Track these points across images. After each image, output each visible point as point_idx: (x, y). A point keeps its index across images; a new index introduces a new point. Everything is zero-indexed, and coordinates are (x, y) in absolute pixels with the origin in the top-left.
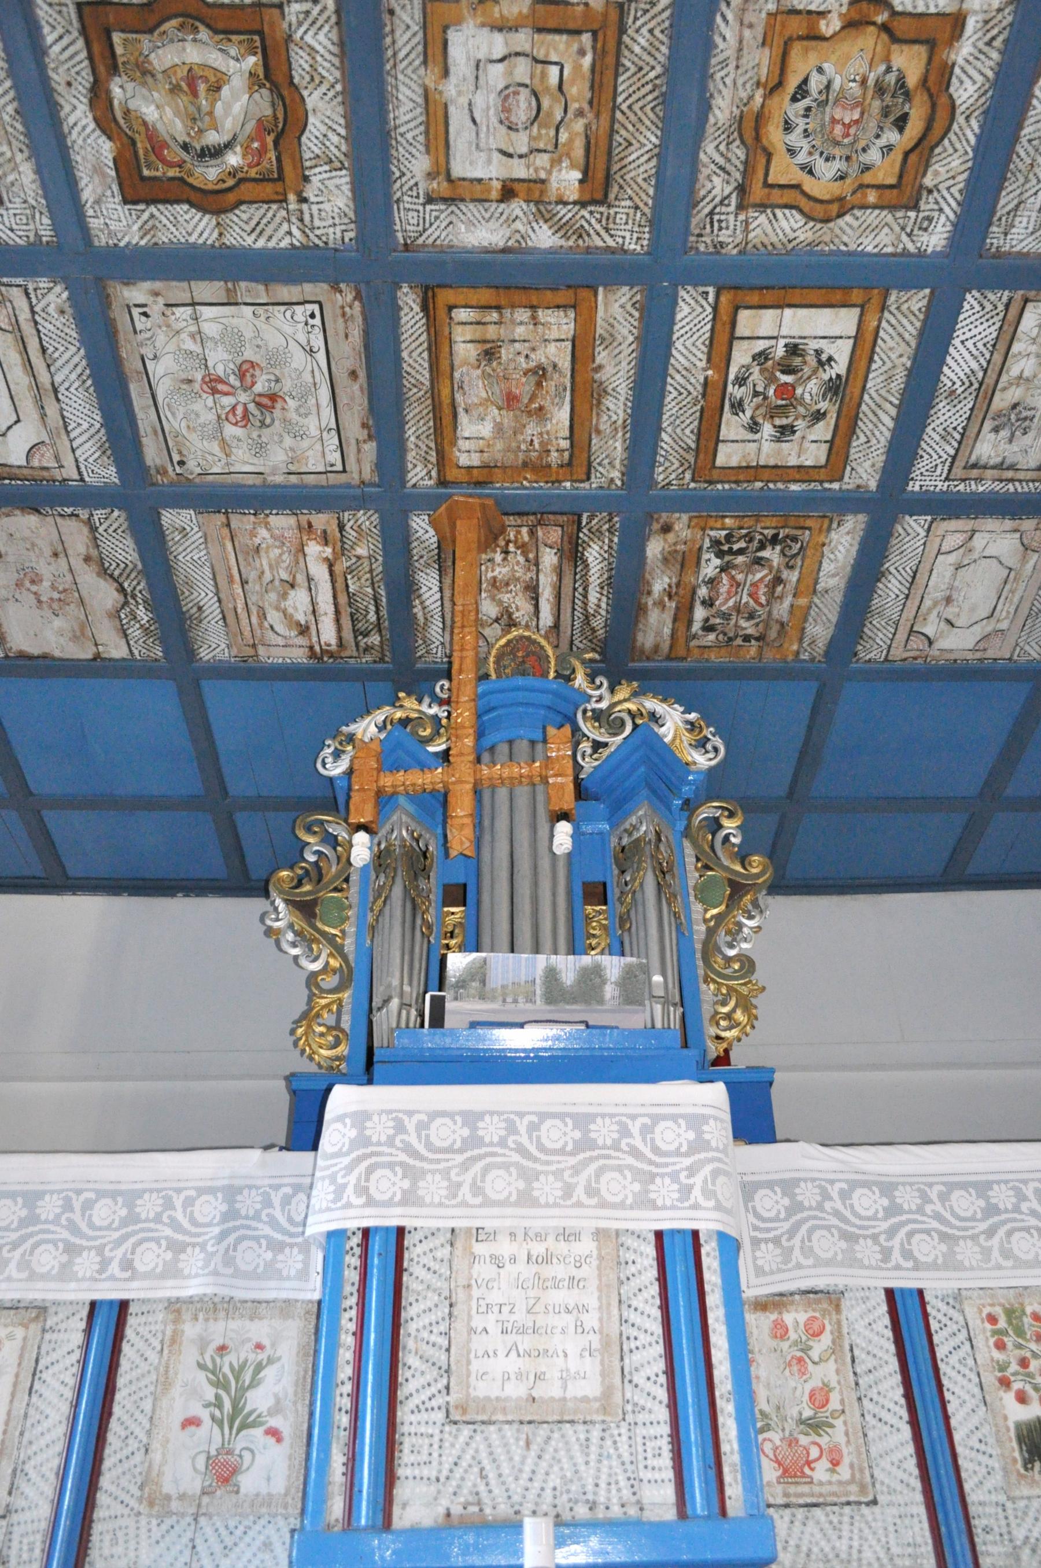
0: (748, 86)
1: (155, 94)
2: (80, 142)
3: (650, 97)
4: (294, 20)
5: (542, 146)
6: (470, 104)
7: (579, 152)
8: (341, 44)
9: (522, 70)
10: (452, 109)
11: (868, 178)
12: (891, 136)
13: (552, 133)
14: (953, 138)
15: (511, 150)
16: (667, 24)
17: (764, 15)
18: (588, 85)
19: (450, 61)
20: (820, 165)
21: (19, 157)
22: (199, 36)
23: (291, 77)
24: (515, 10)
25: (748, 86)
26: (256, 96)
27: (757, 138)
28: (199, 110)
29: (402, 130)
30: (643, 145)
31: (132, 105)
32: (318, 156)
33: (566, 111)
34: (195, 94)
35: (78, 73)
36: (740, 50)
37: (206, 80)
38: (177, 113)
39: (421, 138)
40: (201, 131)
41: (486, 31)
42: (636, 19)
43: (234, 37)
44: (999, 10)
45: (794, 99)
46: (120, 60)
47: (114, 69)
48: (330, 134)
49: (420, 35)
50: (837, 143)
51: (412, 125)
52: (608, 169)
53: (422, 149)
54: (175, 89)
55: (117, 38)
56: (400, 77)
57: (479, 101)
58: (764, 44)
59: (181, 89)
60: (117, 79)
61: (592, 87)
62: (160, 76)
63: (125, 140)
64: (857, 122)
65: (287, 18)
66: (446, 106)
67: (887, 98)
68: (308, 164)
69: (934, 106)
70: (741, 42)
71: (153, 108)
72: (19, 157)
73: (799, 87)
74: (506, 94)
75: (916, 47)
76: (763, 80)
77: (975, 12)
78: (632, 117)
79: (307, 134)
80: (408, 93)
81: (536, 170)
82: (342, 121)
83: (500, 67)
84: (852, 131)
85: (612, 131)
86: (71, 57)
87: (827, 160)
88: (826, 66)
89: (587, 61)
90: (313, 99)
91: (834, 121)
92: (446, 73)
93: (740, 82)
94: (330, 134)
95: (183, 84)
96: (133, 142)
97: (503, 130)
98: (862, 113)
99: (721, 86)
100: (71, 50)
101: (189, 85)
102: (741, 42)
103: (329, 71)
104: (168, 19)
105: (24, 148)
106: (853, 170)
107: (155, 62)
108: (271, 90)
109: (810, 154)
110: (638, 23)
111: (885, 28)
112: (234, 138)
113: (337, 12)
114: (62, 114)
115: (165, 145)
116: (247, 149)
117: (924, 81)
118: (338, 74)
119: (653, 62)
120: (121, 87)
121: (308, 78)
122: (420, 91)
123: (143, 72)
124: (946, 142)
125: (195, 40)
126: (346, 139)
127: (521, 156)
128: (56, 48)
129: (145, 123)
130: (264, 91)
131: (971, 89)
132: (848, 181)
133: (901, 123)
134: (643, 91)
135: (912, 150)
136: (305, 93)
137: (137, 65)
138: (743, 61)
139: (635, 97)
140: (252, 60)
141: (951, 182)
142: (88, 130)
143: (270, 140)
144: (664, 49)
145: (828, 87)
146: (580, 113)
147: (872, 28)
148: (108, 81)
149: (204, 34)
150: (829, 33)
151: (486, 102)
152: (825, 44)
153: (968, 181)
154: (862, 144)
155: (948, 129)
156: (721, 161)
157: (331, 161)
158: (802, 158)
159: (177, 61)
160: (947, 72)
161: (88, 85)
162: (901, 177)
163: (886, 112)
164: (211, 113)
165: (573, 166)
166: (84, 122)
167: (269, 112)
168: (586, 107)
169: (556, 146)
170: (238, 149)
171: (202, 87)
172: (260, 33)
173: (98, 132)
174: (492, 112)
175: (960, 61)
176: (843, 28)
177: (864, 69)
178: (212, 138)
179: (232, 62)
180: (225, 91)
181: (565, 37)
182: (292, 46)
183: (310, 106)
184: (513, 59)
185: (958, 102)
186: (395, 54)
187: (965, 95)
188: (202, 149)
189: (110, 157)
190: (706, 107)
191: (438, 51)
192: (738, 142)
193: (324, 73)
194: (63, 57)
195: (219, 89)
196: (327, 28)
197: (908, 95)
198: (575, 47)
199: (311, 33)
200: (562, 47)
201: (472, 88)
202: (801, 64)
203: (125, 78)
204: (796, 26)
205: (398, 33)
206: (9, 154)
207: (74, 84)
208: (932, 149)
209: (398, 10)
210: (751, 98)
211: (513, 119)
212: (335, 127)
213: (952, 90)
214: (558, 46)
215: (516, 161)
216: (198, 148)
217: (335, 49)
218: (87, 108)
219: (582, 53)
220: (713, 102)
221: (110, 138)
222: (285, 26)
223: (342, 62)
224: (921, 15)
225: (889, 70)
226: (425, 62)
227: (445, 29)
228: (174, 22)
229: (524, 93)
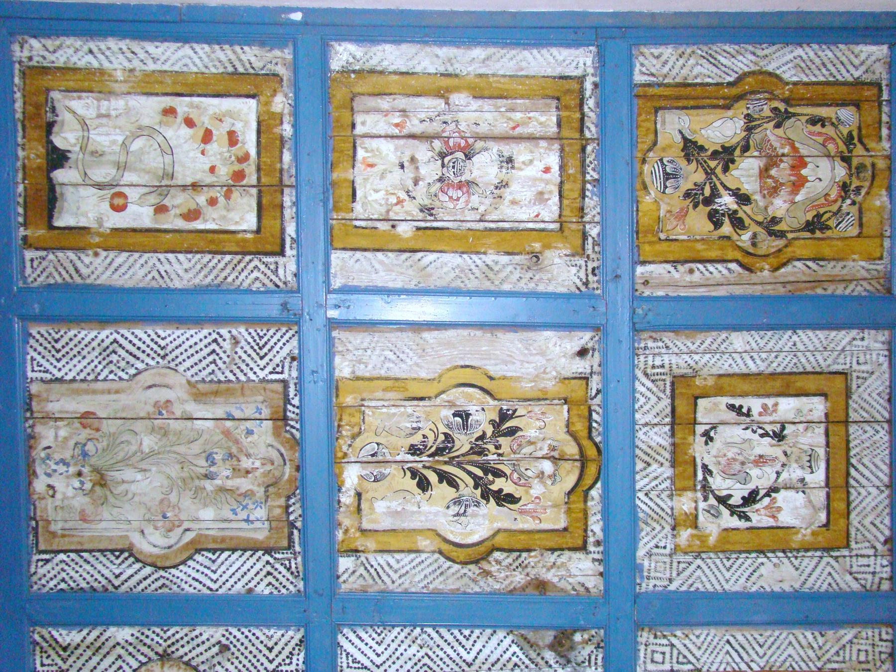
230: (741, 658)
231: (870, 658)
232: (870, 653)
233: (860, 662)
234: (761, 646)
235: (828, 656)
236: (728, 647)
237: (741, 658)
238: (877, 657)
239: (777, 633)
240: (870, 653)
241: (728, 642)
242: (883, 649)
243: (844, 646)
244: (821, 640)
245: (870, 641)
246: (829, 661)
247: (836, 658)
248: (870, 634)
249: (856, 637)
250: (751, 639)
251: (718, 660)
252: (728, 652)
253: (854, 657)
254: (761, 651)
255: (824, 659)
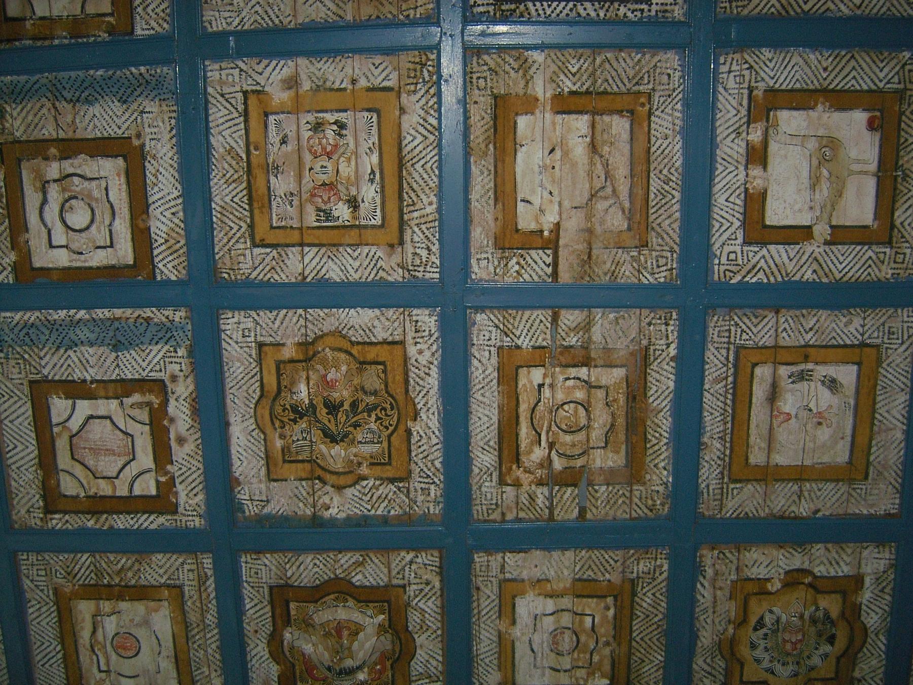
0: (723, 623)
1: (313, 638)
2: (257, 666)
3: (656, 632)
4: (412, 594)
5: (581, 664)
6: (530, 641)
7: (607, 667)
8: (442, 607)
9: (566, 620)
10: (517, 644)
11: (813, 675)
12: (828, 648)
13: (588, 656)
14: (870, 647)
15: (559, 667)
16: (664, 590)
17: (729, 582)
18: (612, 627)
19: (517, 616)
20: (778, 668)
21: (213, 674)
22: (347, 604)
23: (407, 627)
24: (561, 585)
25: (723, 623)
26: (382, 638)
27: (733, 654)
28: (341, 646)
29: (482, 657)
30: (652, 661)
31: (296, 644)
32: (421, 674)
33: (597, 643)
34: (340, 636)
35: (263, 625)
36: (715, 602)
37: (349, 629)
38: (326, 649)
39: (495, 662)
40: (341, 659)
41: (541, 598)
42: (643, 588)
43: (370, 605)
44: (884, 572)
45: (755, 629)
46: (293, 618)
47: (288, 622)
48: (431, 660)
49: (497, 601)
50: (788, 654)
51: (489, 654)
52: (628, 677)
53: (496, 668)
54: (327, 635)
55: (292, 605)
56: (482, 625)
57: (537, 638)
58: (730, 598)
59: (331, 634)
60: (289, 629)
61: (615, 628)
62: (318, 627)
63: (288, 664)
64: (800, 641)
65: (408, 593)
66: (513, 641)
67: (820, 626)
68: (414, 678)
69: (852, 629)
70: (715, 597)
71: (310, 645)
72: (213, 674)
73: (758, 622)
74: (555, 635)
75: (833, 595)
76: (733, 618)
77: (869, 574)
78: (644, 645)
79: (415, 660)
80: (487, 635)
81: (577, 679)
82: (440, 652)
83: (551, 618)
84: (798, 646)
85: (630, 654)
86: (260, 616)
87: (783, 664)
88: (774, 609)
89: (611, 612)
90: (420, 640)
91: (784, 641)
92: (514, 622)
93: (717, 621)
94: (431, 660)
95: (333, 631)
96: (293, 666)
97: (553, 655)
98: (804, 636)
99: (704, 624)
100: (261, 612)
101: (336, 632)
102: (715, 597)
103: (434, 622)
104: (329, 594)
105: (218, 669)
106: (803, 670)
107: (316, 620)
108: (393, 635)
109: (771, 661)
110: (644, 590)
111: (810, 585)
112: (364, 663)
113: (441, 589)
114: (248, 649)
115: (315, 667)
116: (372, 670)
117: (843, 614)
118: (439, 625)
119: (655, 611)
120: (291, 633)
121: (418, 627)
122: (496, 633)
123: (307, 625)
124: (865, 650)
125: (344, 606)
126: (442, 663)
127: (565, 671)
128: (251, 611)
129: (304, 655)
130: (388, 635)
131: (876, 618)
132: (800, 677)
133: (831, 640)
134: (651, 629)
135: (842, 656)
136: (416, 636)
137: (304, 621)
138: (718, 608)
139: (645, 633)
140: (383, 616)
141: (874, 674)
142: (264, 659)
143: (388, 664)
144: (663, 604)
145: (778, 621)
146: (607, 644)
147: (802, 586)
148: (283, 631)
149: (351, 603)
150: (775, 589)
151: (541, 639)
152: (771, 596)
153: (885, 673)
154: (806, 654)
155: (865, 642)
156: (708, 669)
157: (431, 676)
158: (766, 664)
159: (330, 618)
160: (857, 609)
161: (269, 632)
162: (837, 672)
163: (820, 634)
164: (349, 648)
165: (603, 676)
166: (262, 654)
167: (389, 647)
168: (611, 640)
169: (591, 664)
170: (366, 670)
171: (346, 633)
172: (388, 602)
173: (271, 660)
174: (545, 645)
175: (864, 601)
176: (783, 587)
177: (801, 609)
178: (349, 663)
179: (368, 619)
180: (361, 635)
181: (595, 600)
182: (410, 609)
183: (418, 643)
184: (560, 613)
185: (868, 626)
186: (479, 612)
187: (872, 622)
188: (341, 670)
189: (276, 675)
190: (694, 637)
191: (509, 609)
192: (719, 657)
193: (430, 624)
194: (254, 617)
195: (357, 634)
196: (434, 598)
197: (833, 623)
198: (603, 605)
199: (423, 601)
200: (593, 605)
201: (532, 631)
202: (757, 609)
203: (294, 628)
204: (750, 588)
205: (481, 601)
206: (207, 673)
207: (260, 631)
208: (856, 654)
209: (482, 587)
210: (726, 630)
211: (560, 648)
212: (435, 655)
213: (862, 618)
214: (591, 605)
215: (562, 673)
216: (338, 669)
217: (439, 611)
218: (265, 646)
219: (607, 608)
220: (700, 634)
221: (278, 663)
222: (406, 597)
223: (442, 617)
224: (832, 578)
225: (817, 609)
226: (500, 617)
227: (514, 597)
228: (332, 596)
229: (567, 635)
230: (53, 657)
231: (43, 567)
232: (39, 567)
233: (46, 575)
234: (43, 643)
235: (45, 597)
236: (47, 666)
237: (53, 657)
238: (41, 563)
239: (33, 633)
240: (39, 567)
241: (43, 666)
242: (35, 558)
243: (36, 586)
244: (34, 602)
245: (30, 567)
246: (48, 596)
247: (46, 592)
248: (24, 567)
249: (28, 577)
250: (38, 651)
251: (57, 672)
252: (50, 666)
253: (44, 579)
254: (47, 644)
255: (48, 600)
